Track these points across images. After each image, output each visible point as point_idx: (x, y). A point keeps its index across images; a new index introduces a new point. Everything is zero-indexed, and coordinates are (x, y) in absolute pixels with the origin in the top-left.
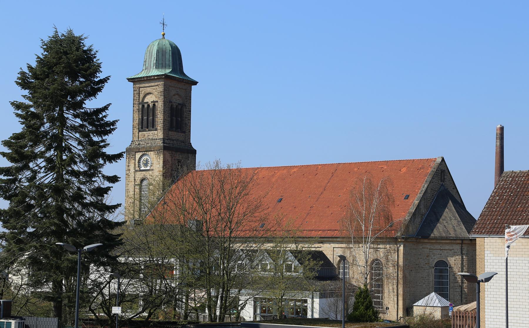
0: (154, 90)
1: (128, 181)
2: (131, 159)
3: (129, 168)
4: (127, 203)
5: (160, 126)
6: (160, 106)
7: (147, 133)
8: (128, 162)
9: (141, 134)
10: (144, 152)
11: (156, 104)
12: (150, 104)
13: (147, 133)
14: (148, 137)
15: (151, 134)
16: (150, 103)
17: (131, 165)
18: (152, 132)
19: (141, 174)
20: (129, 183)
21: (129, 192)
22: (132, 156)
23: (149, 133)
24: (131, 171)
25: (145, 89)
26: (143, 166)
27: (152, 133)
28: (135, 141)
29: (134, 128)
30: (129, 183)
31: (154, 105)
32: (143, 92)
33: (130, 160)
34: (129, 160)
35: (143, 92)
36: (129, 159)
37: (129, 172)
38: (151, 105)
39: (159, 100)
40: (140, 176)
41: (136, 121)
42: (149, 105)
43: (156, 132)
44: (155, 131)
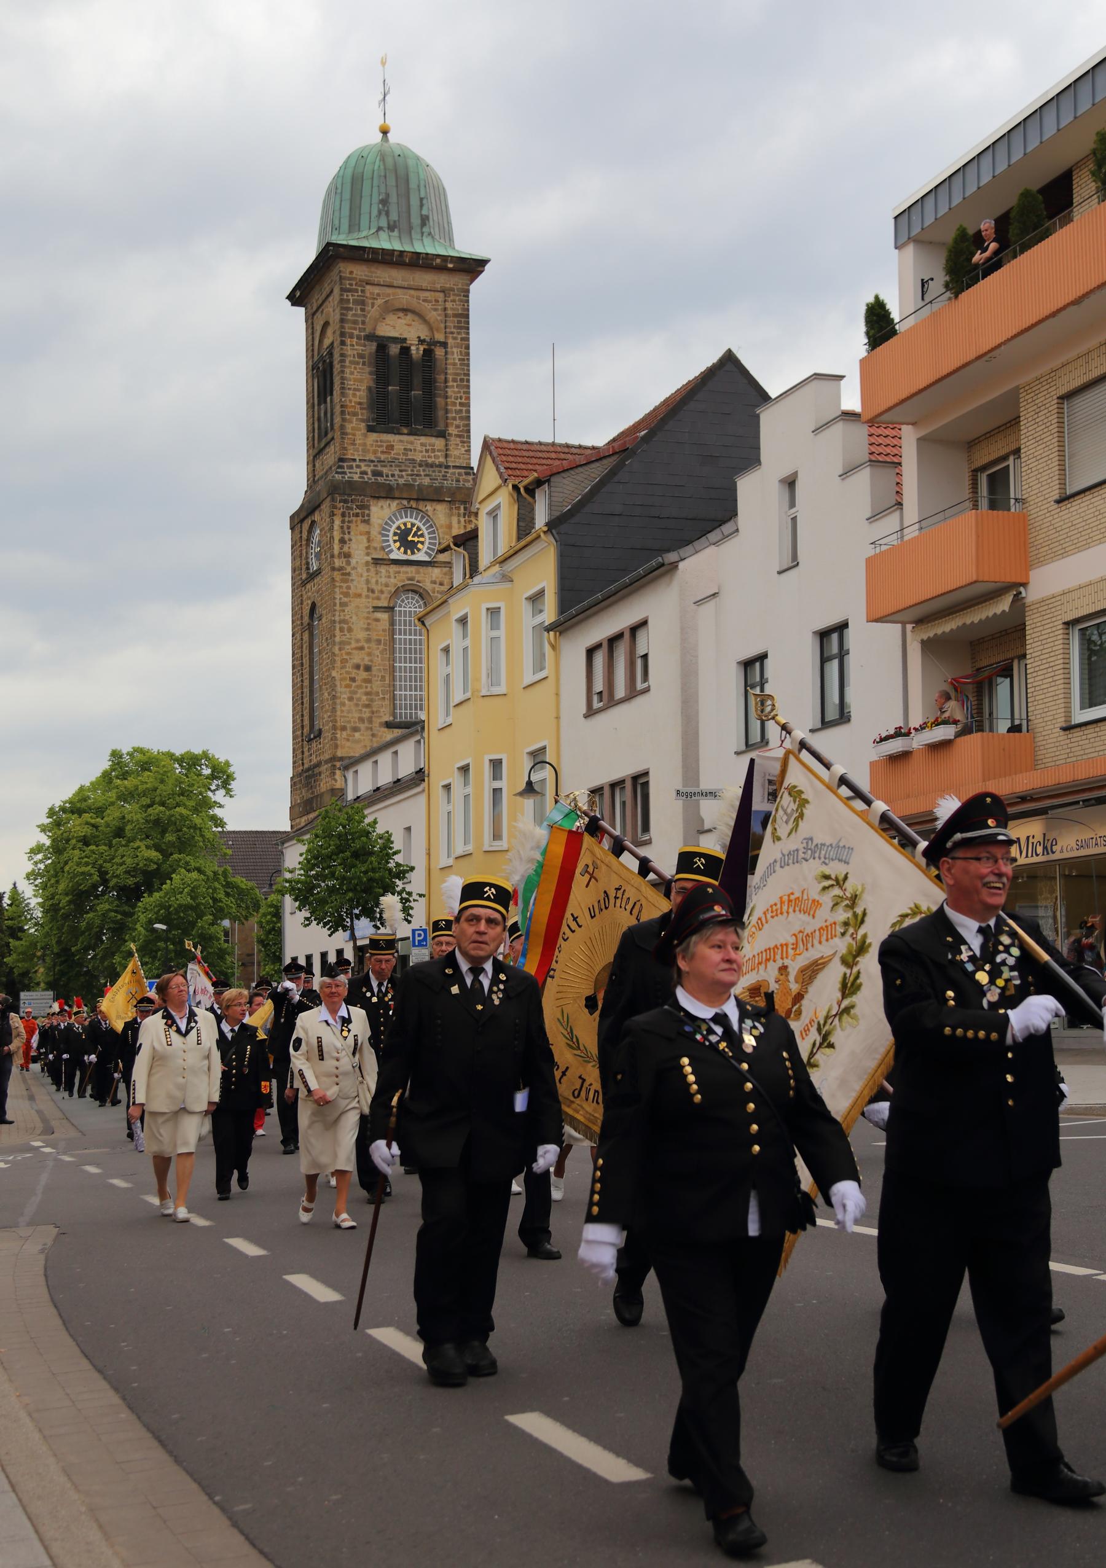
0: (426, 304)
1: (341, 593)
2: (354, 519)
3: (346, 549)
4: (342, 668)
5: (458, 427)
6: (457, 361)
7: (401, 441)
8: (342, 527)
9: (377, 441)
10: (409, 500)
11: (439, 352)
12: (413, 348)
13: (401, 441)
14: (406, 455)
15: (419, 448)
16: (412, 344)
17: (353, 538)
18: (423, 439)
19: (399, 572)
20: (345, 600)
21: (350, 630)
22: (358, 511)
23: (412, 443)
24: (353, 561)
25: (389, 295)
26: (399, 549)
27: (422, 445)
28: (354, 460)
29: (348, 417)
30: (345, 600)
31: (428, 353)
32: (379, 302)
33: (349, 522)
34: (343, 522)
35: (379, 302)
36: (347, 519)
37: (348, 563)
38: (416, 352)
39: (450, 341)
40: (392, 580)
41: (358, 393)
42: (405, 351)
43: (439, 443)
44: (433, 440)
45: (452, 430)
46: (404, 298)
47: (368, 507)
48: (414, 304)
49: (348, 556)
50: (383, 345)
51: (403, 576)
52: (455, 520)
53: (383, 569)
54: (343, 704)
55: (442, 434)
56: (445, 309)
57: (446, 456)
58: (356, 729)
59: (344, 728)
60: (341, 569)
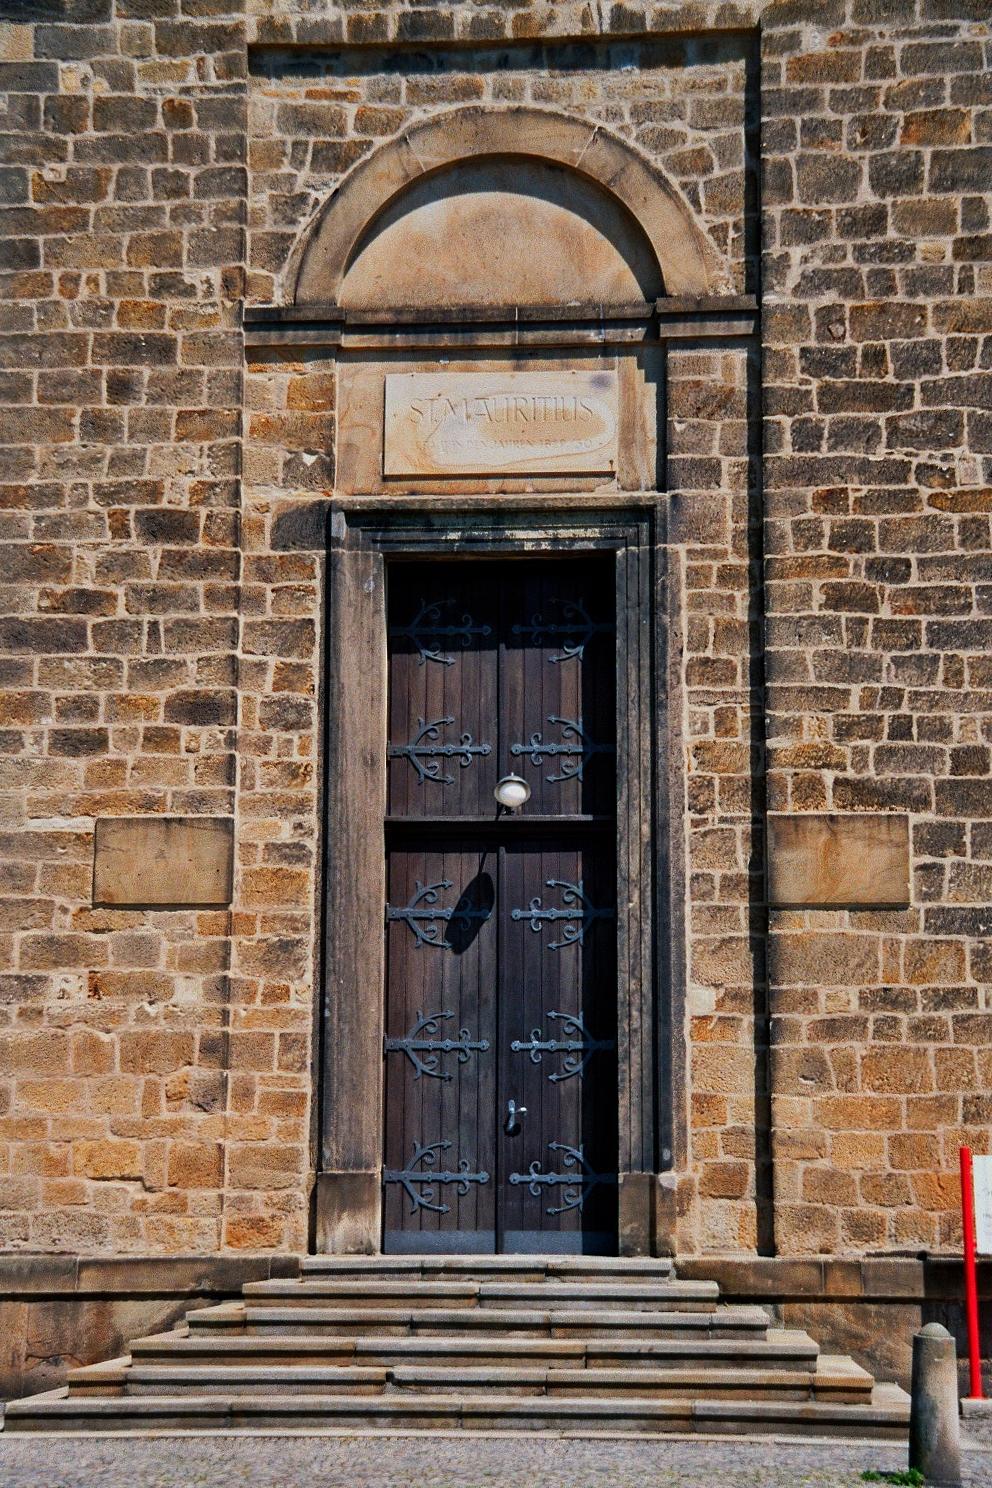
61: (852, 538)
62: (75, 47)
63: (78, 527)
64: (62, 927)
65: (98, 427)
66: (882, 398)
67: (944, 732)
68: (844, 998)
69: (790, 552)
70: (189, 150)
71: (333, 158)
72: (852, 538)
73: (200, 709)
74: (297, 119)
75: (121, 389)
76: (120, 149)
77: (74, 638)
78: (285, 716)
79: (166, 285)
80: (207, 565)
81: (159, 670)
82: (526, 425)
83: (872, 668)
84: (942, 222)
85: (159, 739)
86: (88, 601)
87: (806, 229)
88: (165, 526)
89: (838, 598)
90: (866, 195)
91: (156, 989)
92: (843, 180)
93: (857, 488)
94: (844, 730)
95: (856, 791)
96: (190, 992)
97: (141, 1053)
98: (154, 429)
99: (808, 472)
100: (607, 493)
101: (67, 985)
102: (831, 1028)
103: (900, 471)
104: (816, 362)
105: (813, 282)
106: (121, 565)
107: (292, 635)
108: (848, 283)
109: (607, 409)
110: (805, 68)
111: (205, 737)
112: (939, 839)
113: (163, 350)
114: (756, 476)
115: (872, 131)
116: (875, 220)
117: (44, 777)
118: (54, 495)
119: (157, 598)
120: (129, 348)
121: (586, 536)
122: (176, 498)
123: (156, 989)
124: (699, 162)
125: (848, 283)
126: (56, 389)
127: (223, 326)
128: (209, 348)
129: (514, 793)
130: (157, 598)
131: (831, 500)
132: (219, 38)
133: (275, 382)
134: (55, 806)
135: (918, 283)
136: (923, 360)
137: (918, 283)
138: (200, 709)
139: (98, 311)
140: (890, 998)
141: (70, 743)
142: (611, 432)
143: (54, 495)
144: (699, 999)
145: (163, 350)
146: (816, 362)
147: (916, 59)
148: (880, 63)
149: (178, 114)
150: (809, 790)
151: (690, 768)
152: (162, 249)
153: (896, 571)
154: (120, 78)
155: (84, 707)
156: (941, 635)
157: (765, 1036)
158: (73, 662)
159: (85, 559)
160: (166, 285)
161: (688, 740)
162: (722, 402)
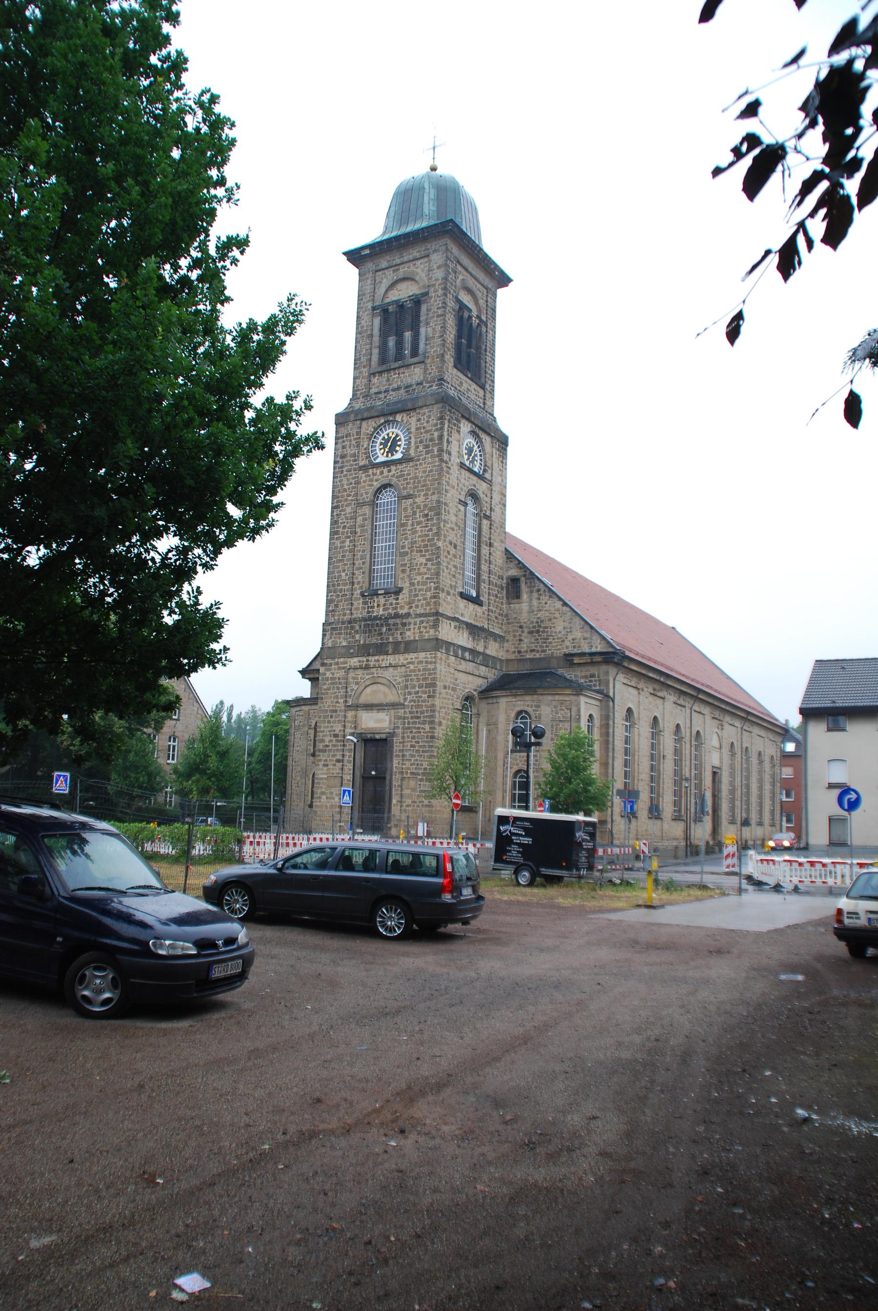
20: (448, 487)
45: (487, 386)
46: (471, 283)
47: (459, 422)
48: (474, 289)
49: (450, 454)
50: (462, 307)
51: (471, 482)
52: (494, 450)
53: (463, 471)
54: (443, 571)
55: (483, 387)
56: (487, 301)
57: (484, 404)
58: (448, 593)
59: (443, 591)
60: (446, 463)
61: (413, 738)
62: (328, 670)
63: (326, 736)
64: (323, 790)
65: (329, 722)
66: (418, 718)
67: (422, 765)
68: (409, 802)
69: (406, 740)
70: (340, 683)
71: (357, 683)
72: (413, 738)
73: (338, 761)
74: (353, 678)
75: (331, 717)
76: (332, 684)
77: (325, 751)
78: (349, 762)
79: (337, 702)
80: (340, 741)
81: (334, 756)
82: (378, 721)
83: (414, 756)
84: (426, 693)
85: (334, 765)
86: (327, 746)
87: (410, 693)
88: (336, 736)
89: (412, 746)
90: (417, 689)
91: (333, 798)
92: (414, 687)
93: (414, 731)
94: (411, 765)
95: (412, 773)
96: (337, 799)
97: (332, 806)
98: (334, 722)
99: (409, 728)
100: (387, 730)
101: (324, 797)
102: (407, 806)
103: (419, 728)
104: (411, 713)
105: (410, 701)
106: (331, 741)
107: (350, 750)
108: (414, 701)
109: (387, 718)
110: (411, 671)
111: (339, 765)
112: (421, 780)
113: (336, 711)
114: (403, 728)
115: (418, 680)
116: (418, 692)
117: (322, 770)
118: (323, 731)
119: (334, 746)
120: (333, 711)
121: (384, 736)
122: (337, 732)
123: (333, 798)
124: (399, 683)
125: (414, 701)
126: (325, 717)
127: (343, 708)
128: (341, 711)
129: (373, 773)
130: (334, 746)
131: (411, 732)
132: (344, 668)
133: (350, 714)
134: (322, 774)
135: (423, 701)
136: (422, 712)
137: (423, 701)
138: (338, 761)
139: (329, 706)
140: (414, 802)
141: (325, 765)
142: (388, 722)
143: (323, 731)
144: (394, 801)
145: (336, 711)
146: (411, 713)
147: (424, 670)
148: (419, 670)
149: (339, 679)
150: (407, 773)
151: (395, 770)
152: (337, 697)
153: (418, 742)
154: (333, 674)
155: (326, 761)
156: (423, 751)
157: (401, 806)
158: (325, 754)
159: (327, 739)
160: (337, 702)
161: (394, 765)
162: (400, 718)
